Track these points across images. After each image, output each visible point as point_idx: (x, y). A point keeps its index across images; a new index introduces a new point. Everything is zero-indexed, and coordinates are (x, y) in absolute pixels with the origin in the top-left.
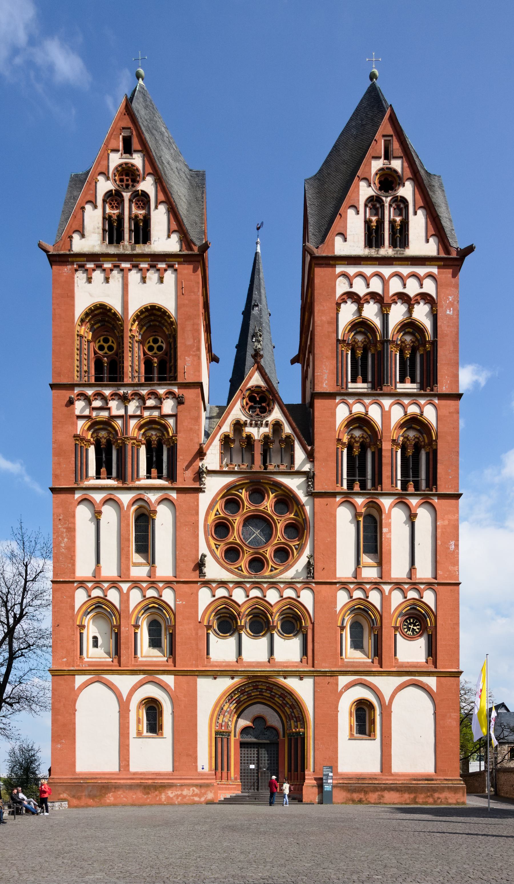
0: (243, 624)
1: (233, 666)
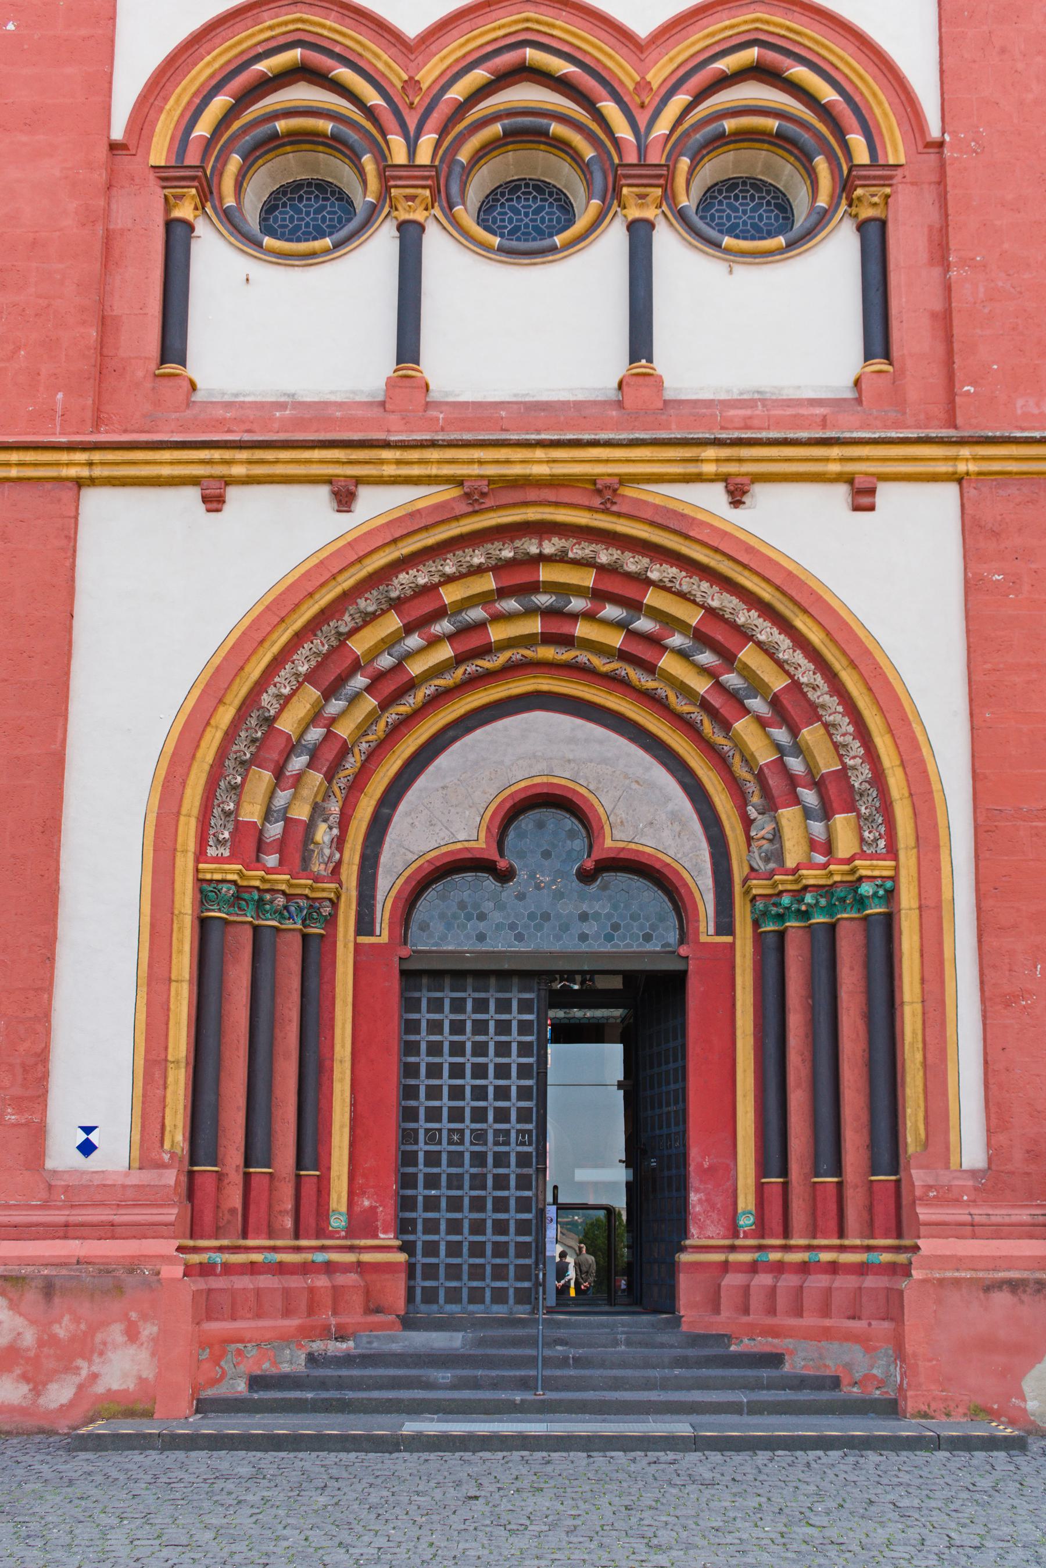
0: (424, 157)
1: (349, 422)
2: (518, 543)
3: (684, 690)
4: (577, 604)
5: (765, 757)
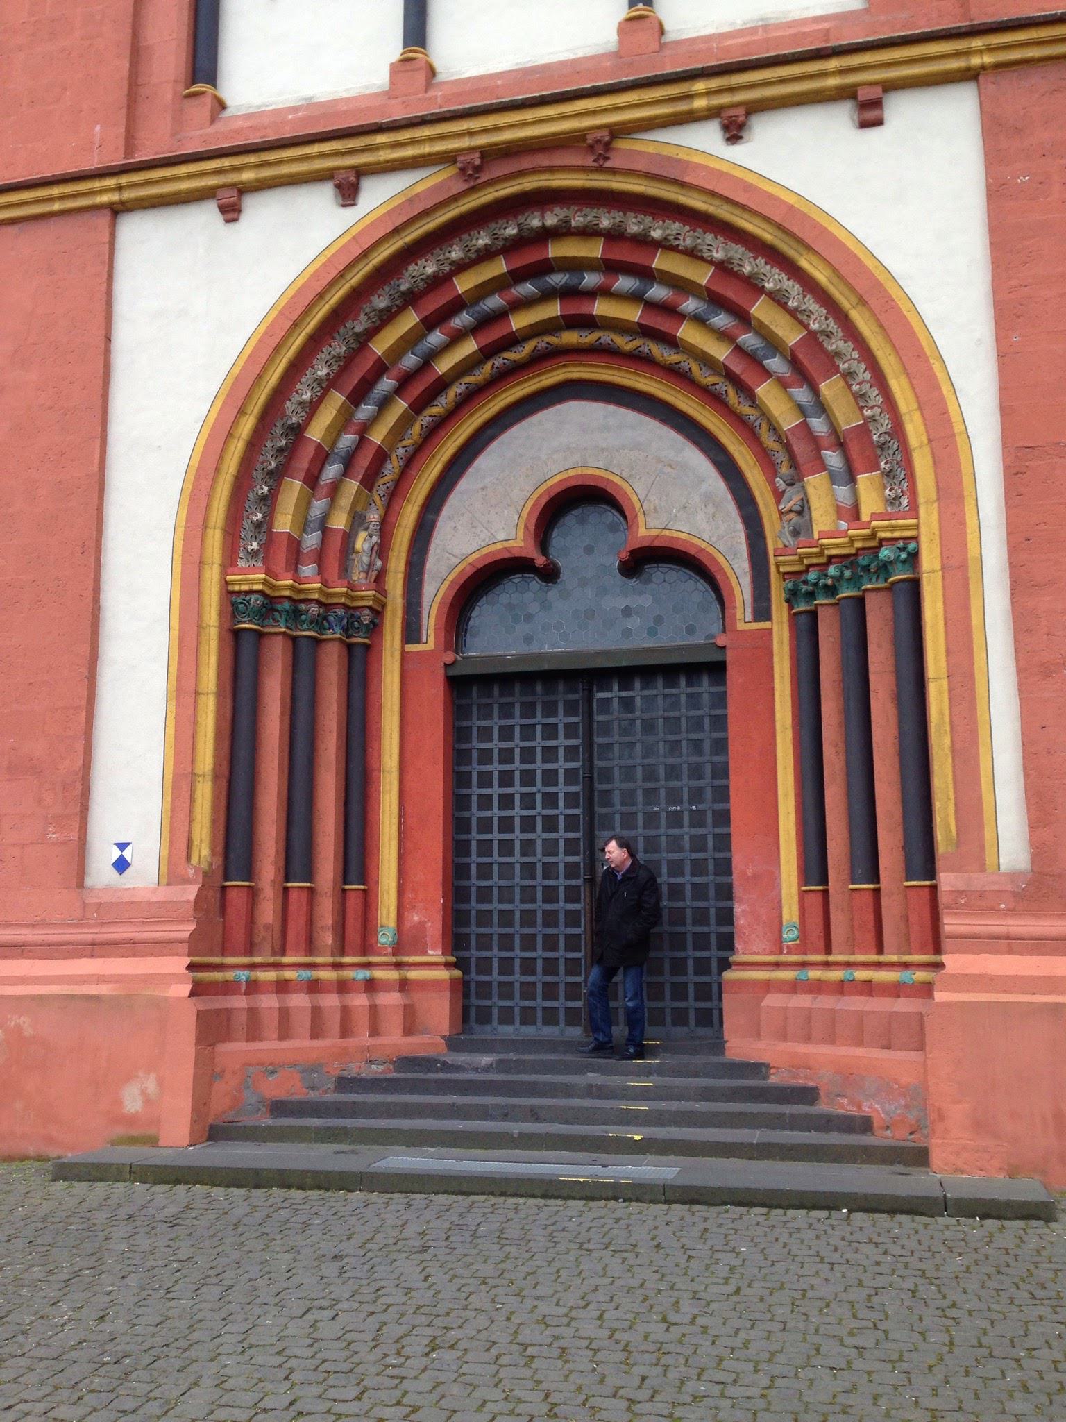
2: (521, 219)
3: (706, 361)
4: (591, 280)
5: (788, 421)
